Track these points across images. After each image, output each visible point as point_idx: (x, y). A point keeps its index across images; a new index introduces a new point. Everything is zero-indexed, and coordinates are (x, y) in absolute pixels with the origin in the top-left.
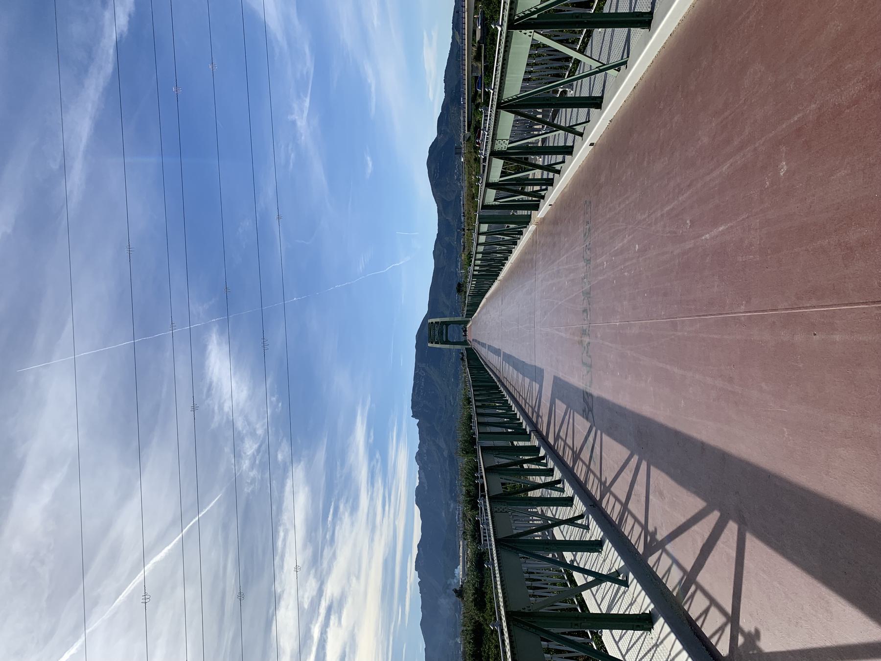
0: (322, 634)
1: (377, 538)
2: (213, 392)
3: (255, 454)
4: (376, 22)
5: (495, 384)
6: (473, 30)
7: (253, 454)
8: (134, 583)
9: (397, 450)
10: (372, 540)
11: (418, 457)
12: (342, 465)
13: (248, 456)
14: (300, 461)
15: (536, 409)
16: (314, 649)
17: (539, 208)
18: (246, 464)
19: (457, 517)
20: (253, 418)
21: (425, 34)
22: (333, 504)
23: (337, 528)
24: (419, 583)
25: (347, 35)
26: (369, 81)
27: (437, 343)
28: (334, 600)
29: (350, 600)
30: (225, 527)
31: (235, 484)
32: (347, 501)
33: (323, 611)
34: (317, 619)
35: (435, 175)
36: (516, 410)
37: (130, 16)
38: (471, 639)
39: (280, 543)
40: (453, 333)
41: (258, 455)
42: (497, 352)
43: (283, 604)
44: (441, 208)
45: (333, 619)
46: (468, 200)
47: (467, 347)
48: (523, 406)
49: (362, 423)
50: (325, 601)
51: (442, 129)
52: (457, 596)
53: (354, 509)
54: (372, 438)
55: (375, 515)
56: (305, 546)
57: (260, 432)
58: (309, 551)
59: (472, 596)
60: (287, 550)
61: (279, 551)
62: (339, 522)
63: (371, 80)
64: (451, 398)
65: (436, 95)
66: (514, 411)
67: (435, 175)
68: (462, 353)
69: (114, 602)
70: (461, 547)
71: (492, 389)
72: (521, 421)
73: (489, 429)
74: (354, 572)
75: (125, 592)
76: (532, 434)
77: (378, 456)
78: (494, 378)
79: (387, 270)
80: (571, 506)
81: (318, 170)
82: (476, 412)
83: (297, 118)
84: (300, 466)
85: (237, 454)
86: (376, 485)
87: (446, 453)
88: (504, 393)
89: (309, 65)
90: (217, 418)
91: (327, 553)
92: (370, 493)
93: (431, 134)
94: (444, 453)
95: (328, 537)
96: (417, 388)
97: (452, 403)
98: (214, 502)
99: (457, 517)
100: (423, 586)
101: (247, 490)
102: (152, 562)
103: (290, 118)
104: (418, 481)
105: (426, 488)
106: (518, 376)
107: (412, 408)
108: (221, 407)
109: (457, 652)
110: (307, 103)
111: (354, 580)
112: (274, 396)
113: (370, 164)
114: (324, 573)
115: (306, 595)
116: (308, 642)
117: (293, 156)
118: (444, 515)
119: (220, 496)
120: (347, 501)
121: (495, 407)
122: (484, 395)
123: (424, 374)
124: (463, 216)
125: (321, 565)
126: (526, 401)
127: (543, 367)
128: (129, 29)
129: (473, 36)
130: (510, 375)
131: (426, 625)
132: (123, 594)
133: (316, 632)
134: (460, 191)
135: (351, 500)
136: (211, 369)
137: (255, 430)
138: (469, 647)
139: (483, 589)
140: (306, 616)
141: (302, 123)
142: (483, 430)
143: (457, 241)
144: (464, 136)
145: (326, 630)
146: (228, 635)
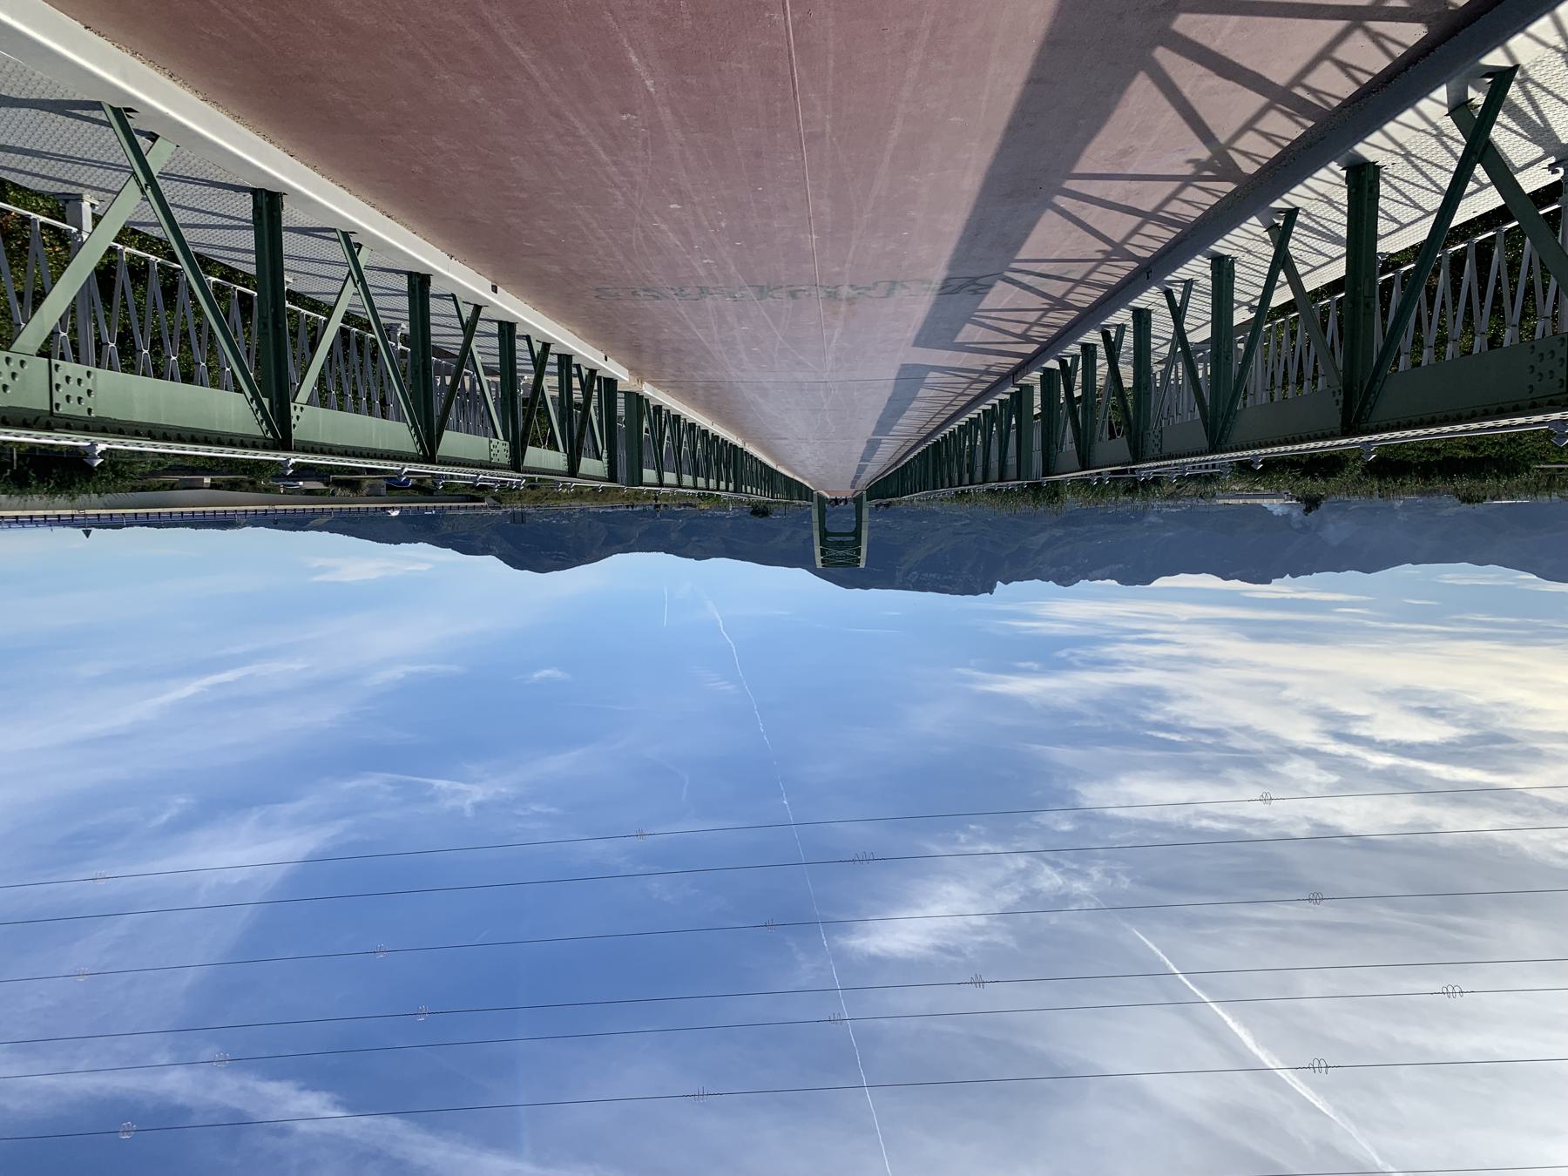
1: (1212, 654)
2: (952, 944)
3: (1060, 870)
4: (298, 666)
5: (930, 450)
6: (306, 494)
7: (1062, 873)
8: (1293, 1082)
10: (1214, 662)
11: (1065, 582)
12: (1081, 716)
13: (1064, 883)
14: (1073, 792)
15: (975, 376)
16: (1413, 763)
17: (611, 379)
18: (1080, 886)
19: (1174, 510)
20: (998, 874)
21: (317, 579)
22: (1150, 733)
23: (1193, 724)
24: (1293, 577)
25: (324, 715)
26: (402, 676)
27: (858, 552)
28: (1325, 729)
29: (1324, 701)
30: (1192, 922)
31: (1116, 907)
32: (1146, 708)
33: (1342, 749)
34: (1358, 758)
35: (561, 557)
36: (976, 411)
37: (302, 1089)
38: (1396, 481)
39: (1221, 826)
40: (841, 523)
41: (1062, 866)
42: (873, 446)
43: (1330, 820)
44: (619, 547)
45: (1358, 730)
46: (604, 500)
47: (865, 497)
48: (970, 398)
49: (1005, 682)
51: (482, 546)
52: (1317, 508)
53: (1158, 694)
55: (1169, 658)
56: (1228, 782)
57: (1021, 862)
58: (1237, 774)
59: (1316, 480)
60: (1233, 813)
61: (1234, 826)
63: (398, 672)
64: (959, 524)
65: (423, 558)
66: (979, 414)
67: (561, 557)
68: (877, 506)
69: (1327, 1115)
70: (1227, 501)
71: (940, 454)
72: (997, 402)
73: (1012, 461)
74: (1273, 693)
75: (1308, 1097)
76: (1020, 382)
77: (1063, 654)
78: (920, 450)
79: (730, 642)
80: (1150, 312)
81: (558, 764)
82: (980, 484)
83: (468, 802)
84: (1083, 792)
85: (1062, 901)
86: (1116, 657)
87: (1058, 532)
88: (946, 431)
89: (378, 782)
90: (998, 938)
91: (1240, 741)
92: (1130, 667)
93: (490, 565)
94: (1058, 535)
95: (1209, 741)
96: (941, 586)
97: (968, 521)
98: (1147, 942)
99: (1174, 510)
100: (1298, 568)
101: (1125, 883)
102: (1255, 1050)
103: (469, 813)
104: (1108, 581)
105: (1121, 566)
106: (916, 409)
107: (976, 593)
108: (978, 931)
109: (1418, 507)
110: (442, 784)
111: (1287, 694)
112: (956, 840)
113: (546, 672)
114: (1274, 747)
115: (1314, 777)
116: (1400, 774)
117: (536, 808)
118: (1171, 534)
119: (1137, 933)
120: (1146, 708)
121: (973, 447)
122: (950, 469)
123: (915, 573)
124: (632, 507)
125: (1260, 752)
126: (960, 395)
127: (897, 365)
128: (327, 1090)
129: (317, 495)
130: (913, 424)
131: (1370, 564)
132: (1312, 1100)
134: (589, 512)
135: (1145, 701)
136: (910, 948)
137: (1019, 871)
138: (1411, 483)
139: (1304, 461)
140: (1352, 777)
141: (478, 793)
142: (1012, 472)
143: (679, 518)
144: (493, 508)
145: (1378, 743)
146: (1385, 914)
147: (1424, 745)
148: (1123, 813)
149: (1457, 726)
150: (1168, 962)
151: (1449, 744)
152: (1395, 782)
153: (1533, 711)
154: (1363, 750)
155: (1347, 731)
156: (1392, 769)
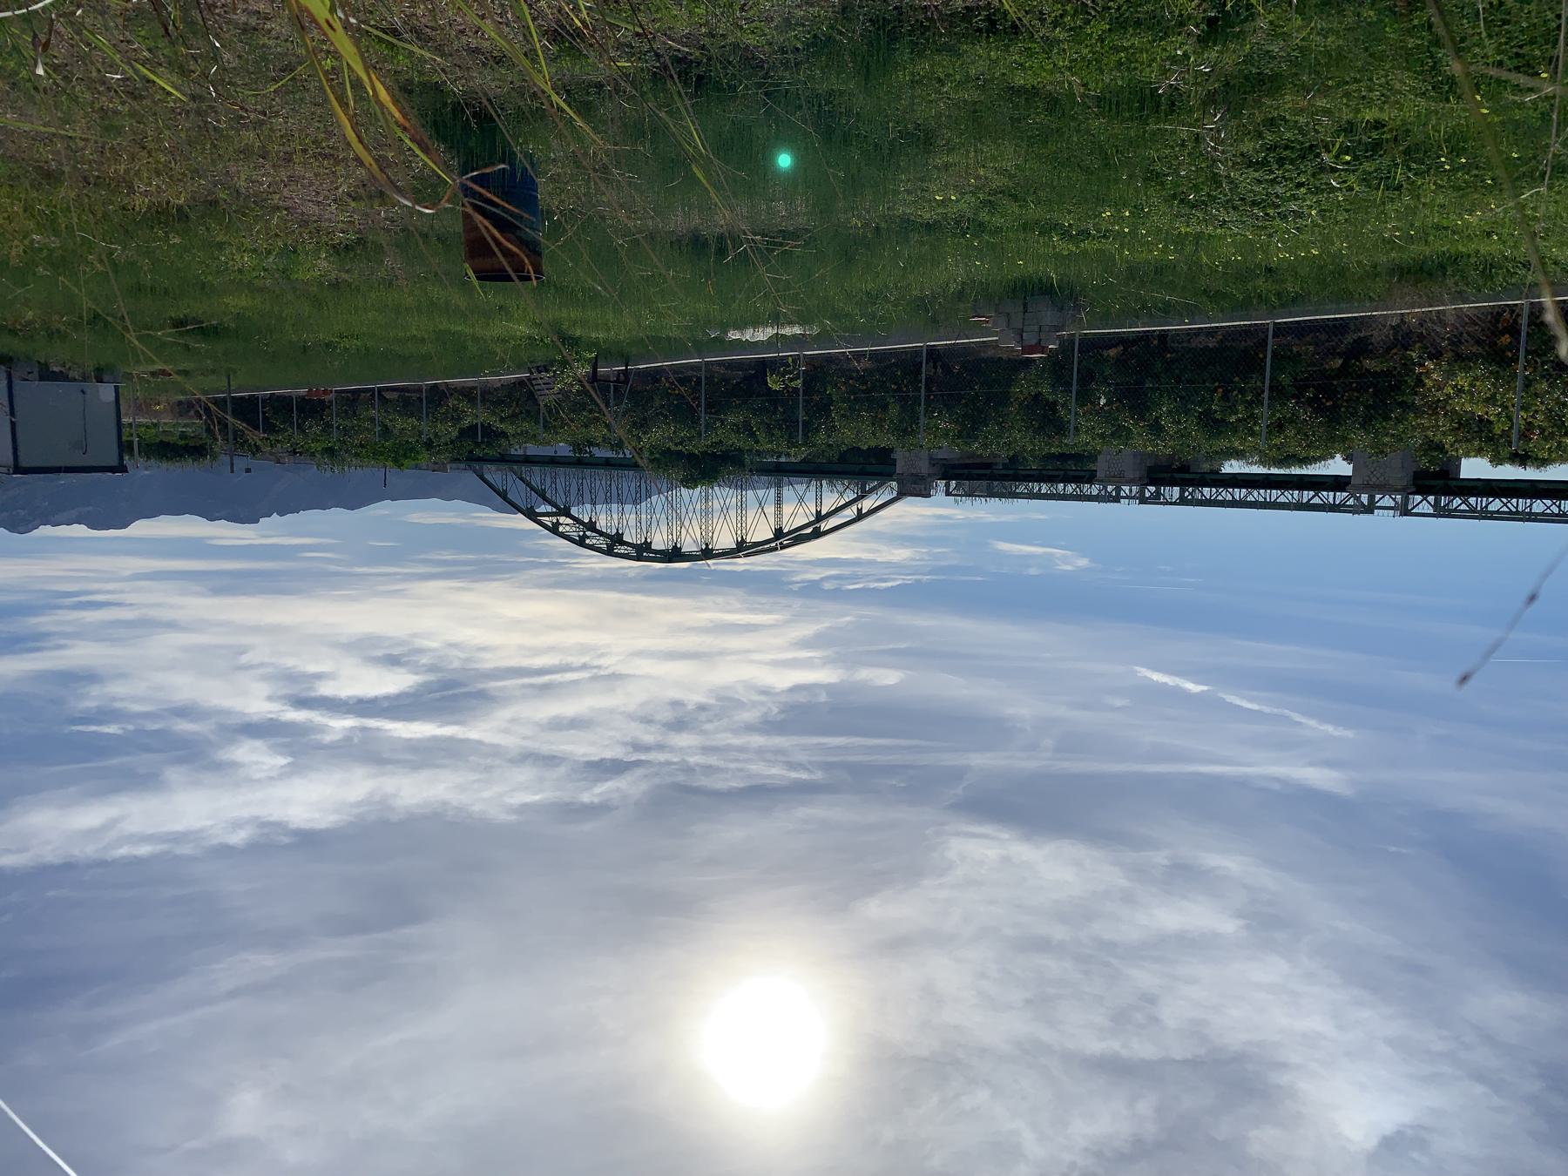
16: (372, 723)
29: (290, 662)
45: (326, 689)
62: (118, 705)
86: (43, 629)
145: (354, 704)
147: (387, 698)
149: (416, 674)
154: (322, 715)
155: (304, 694)
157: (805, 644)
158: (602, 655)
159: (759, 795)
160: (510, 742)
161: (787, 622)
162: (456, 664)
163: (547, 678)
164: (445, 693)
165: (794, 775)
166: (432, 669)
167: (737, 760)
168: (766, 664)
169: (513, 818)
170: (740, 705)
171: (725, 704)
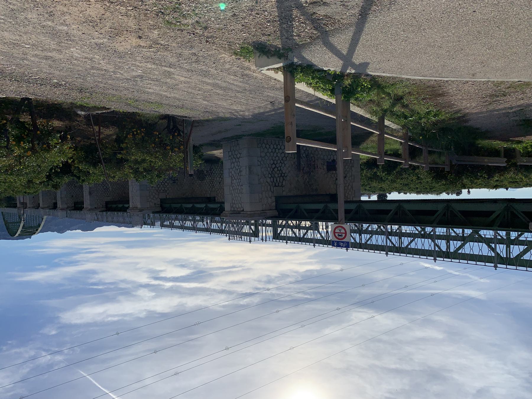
0: (170, 281)
9: (51, 248)
16: (178, 284)
22: (91, 287)
29: (151, 267)
34: (161, 285)
43: (152, 309)
45: (162, 275)
50: (150, 281)
54: (42, 266)
56: (118, 302)
58: (121, 298)
91: (122, 286)
111: (138, 266)
133: (169, 284)
140: (159, 291)
147: (181, 277)
148: (78, 322)
149: (190, 269)
150: (92, 380)
151: (188, 275)
152: (173, 291)
153: (210, 262)
154: (163, 282)
155: (158, 276)
156: (172, 287)
157: (310, 257)
158: (246, 263)
159: (296, 302)
160: (219, 288)
161: (305, 251)
162: (202, 266)
163: (228, 270)
164: (199, 275)
165: (306, 296)
166: (195, 268)
167: (287, 292)
168: (298, 264)
169: (222, 309)
170: (288, 276)
171: (283, 276)
